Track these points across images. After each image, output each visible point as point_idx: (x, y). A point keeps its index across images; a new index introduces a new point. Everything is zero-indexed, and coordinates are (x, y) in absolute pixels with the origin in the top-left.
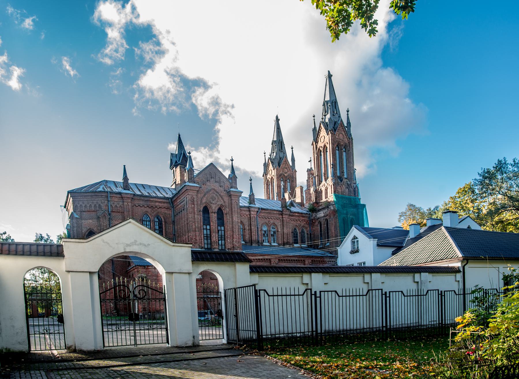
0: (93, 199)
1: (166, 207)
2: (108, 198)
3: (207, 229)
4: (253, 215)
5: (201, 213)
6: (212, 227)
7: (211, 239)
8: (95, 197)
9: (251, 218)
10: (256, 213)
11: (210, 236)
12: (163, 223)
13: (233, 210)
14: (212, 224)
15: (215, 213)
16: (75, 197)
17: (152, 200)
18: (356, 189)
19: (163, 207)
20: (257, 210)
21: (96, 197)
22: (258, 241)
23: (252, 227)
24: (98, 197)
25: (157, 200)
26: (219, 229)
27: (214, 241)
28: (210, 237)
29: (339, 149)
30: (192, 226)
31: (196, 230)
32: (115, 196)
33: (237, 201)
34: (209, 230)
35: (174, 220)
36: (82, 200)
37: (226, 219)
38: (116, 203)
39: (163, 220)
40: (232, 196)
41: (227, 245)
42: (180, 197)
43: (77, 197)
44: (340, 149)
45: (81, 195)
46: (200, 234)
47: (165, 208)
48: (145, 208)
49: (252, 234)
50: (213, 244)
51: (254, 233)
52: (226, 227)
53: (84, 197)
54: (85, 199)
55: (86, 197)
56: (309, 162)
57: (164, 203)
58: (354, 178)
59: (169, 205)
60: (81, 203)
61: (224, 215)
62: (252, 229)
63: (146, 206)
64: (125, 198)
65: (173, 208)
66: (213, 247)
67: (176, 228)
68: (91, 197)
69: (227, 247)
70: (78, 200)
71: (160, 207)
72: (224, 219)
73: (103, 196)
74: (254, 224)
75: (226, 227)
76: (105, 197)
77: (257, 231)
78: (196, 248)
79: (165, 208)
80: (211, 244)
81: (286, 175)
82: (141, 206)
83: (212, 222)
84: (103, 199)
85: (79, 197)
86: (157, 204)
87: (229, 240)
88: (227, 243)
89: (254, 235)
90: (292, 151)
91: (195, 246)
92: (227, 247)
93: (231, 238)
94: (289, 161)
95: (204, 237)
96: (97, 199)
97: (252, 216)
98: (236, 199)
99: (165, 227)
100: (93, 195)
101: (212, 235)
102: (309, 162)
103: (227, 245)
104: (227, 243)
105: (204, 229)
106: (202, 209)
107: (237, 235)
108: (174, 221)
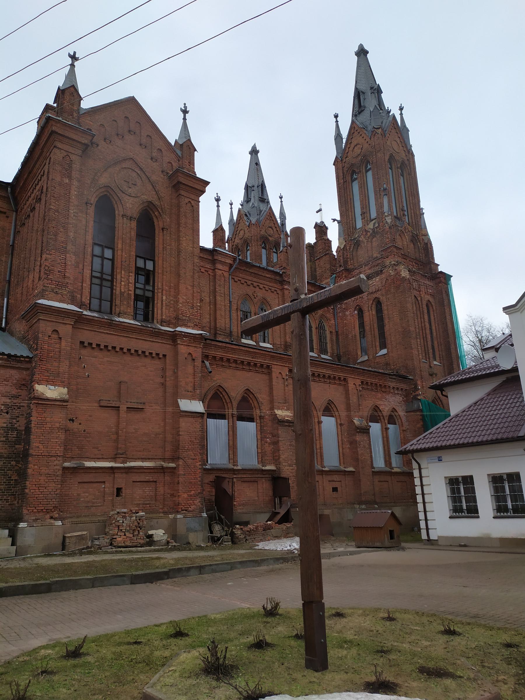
3: (102, 257)
4: (220, 272)
5: (91, 210)
6: (119, 253)
7: (112, 288)
9: (217, 277)
10: (227, 269)
11: (113, 278)
13: (183, 220)
14: (120, 246)
15: (131, 218)
18: (429, 245)
20: (231, 262)
22: (231, 332)
23: (218, 298)
26: (138, 265)
27: (122, 293)
28: (112, 281)
29: (391, 167)
30: (56, 235)
31: (68, 248)
33: (192, 202)
34: (110, 263)
35: (14, 242)
37: (161, 241)
41: (159, 312)
44: (393, 167)
46: (81, 266)
49: (218, 312)
50: (118, 302)
51: (223, 314)
52: (160, 262)
56: (317, 212)
61: (157, 232)
62: (218, 302)
65: (16, 211)
66: (118, 310)
67: (16, 262)
69: (159, 318)
72: (157, 243)
74: (222, 292)
75: (160, 262)
77: (228, 307)
78: (60, 301)
80: (111, 301)
81: (270, 239)
83: (120, 242)
87: (164, 298)
88: (159, 305)
89: (221, 315)
90: (281, 202)
91: (56, 293)
93: (172, 293)
94: (277, 218)
95: (92, 277)
97: (219, 272)
98: (193, 197)
101: (119, 277)
102: (317, 212)
103: (159, 312)
104: (159, 305)
105: (93, 256)
106: (93, 200)
107: (190, 288)
108: (13, 246)
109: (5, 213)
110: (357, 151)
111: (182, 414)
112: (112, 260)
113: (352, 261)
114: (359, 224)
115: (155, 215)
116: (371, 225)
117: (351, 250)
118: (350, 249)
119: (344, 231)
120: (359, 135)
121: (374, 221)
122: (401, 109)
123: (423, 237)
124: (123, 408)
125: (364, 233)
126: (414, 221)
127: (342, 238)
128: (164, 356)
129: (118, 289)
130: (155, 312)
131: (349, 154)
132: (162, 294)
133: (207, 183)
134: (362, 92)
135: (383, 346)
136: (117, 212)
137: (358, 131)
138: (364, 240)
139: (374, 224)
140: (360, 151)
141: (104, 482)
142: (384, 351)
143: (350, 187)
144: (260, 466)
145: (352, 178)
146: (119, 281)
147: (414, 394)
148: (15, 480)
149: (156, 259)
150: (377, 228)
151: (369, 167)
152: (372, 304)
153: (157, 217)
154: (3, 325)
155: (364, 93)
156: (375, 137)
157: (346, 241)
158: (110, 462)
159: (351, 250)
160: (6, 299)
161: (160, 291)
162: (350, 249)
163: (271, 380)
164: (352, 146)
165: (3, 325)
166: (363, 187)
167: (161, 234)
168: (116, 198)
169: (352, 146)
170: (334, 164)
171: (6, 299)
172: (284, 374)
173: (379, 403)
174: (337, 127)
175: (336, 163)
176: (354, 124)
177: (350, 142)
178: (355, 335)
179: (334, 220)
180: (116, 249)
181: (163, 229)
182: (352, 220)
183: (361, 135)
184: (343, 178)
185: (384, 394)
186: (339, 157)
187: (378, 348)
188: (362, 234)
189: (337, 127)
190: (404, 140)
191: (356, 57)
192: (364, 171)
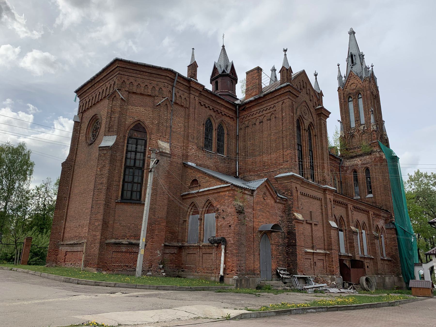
0: (151, 78)
1: (231, 116)
2: (173, 82)
6: (304, 148)
8: (155, 75)
12: (225, 135)
16: (125, 69)
17: (219, 102)
19: (228, 115)
21: (157, 76)
24: (159, 76)
25: (223, 103)
32: (182, 82)
36: (134, 75)
38: (180, 92)
39: (225, 132)
40: (322, 115)
41: (317, 177)
42: (263, 103)
43: (127, 70)
45: (135, 68)
47: (229, 116)
48: (210, 111)
53: (138, 72)
54: (139, 76)
55: (142, 73)
57: (230, 109)
58: (384, 129)
59: (234, 115)
60: (132, 79)
63: (211, 108)
64: (193, 89)
68: (149, 74)
70: (129, 75)
71: (225, 114)
73: (167, 78)
76: (169, 79)
78: (296, 173)
79: (229, 116)
82: (207, 106)
84: (167, 81)
85: (131, 71)
86: (222, 109)
92: (317, 180)
96: (158, 80)
99: (228, 140)
100: (154, 72)
103: (317, 177)
109: (233, 118)
110: (353, 87)
111: (332, 228)
112: (301, 151)
113: (349, 145)
114: (353, 125)
115: (311, 128)
116: (362, 127)
117: (348, 138)
118: (348, 138)
119: (344, 127)
120: (354, 79)
121: (363, 126)
122: (372, 66)
123: (385, 136)
124: (313, 224)
125: (358, 131)
126: (380, 127)
127: (343, 131)
128: (321, 199)
129: (305, 166)
130: (315, 177)
131: (347, 87)
132: (317, 168)
133: (330, 113)
134: (354, 55)
135: (370, 193)
136: (301, 128)
137: (354, 76)
138: (357, 135)
139: (364, 127)
140: (355, 87)
141: (311, 259)
142: (371, 195)
143: (348, 105)
144: (346, 254)
145: (348, 100)
146: (305, 162)
147: (390, 220)
148: (286, 256)
149: (313, 150)
150: (366, 130)
151: (360, 96)
152: (364, 170)
153: (312, 129)
154: (237, 175)
155: (355, 56)
156: (366, 82)
157: (345, 133)
158: (311, 249)
159: (348, 138)
160: (237, 162)
161: (316, 166)
162: (348, 138)
163: (347, 211)
164: (350, 83)
165: (237, 175)
166: (356, 106)
167: (314, 138)
168: (301, 120)
169: (350, 83)
170: (338, 91)
171: (237, 162)
172: (351, 208)
173: (378, 223)
174: (339, 71)
175: (339, 90)
176: (352, 73)
177: (348, 81)
178: (352, 185)
179: (339, 121)
180: (302, 146)
181: (315, 136)
182: (349, 123)
183: (356, 79)
184: (344, 99)
185: (379, 219)
186: (341, 87)
187: (367, 193)
188: (356, 131)
189: (339, 71)
190: (375, 83)
191: (349, 35)
192: (357, 98)
